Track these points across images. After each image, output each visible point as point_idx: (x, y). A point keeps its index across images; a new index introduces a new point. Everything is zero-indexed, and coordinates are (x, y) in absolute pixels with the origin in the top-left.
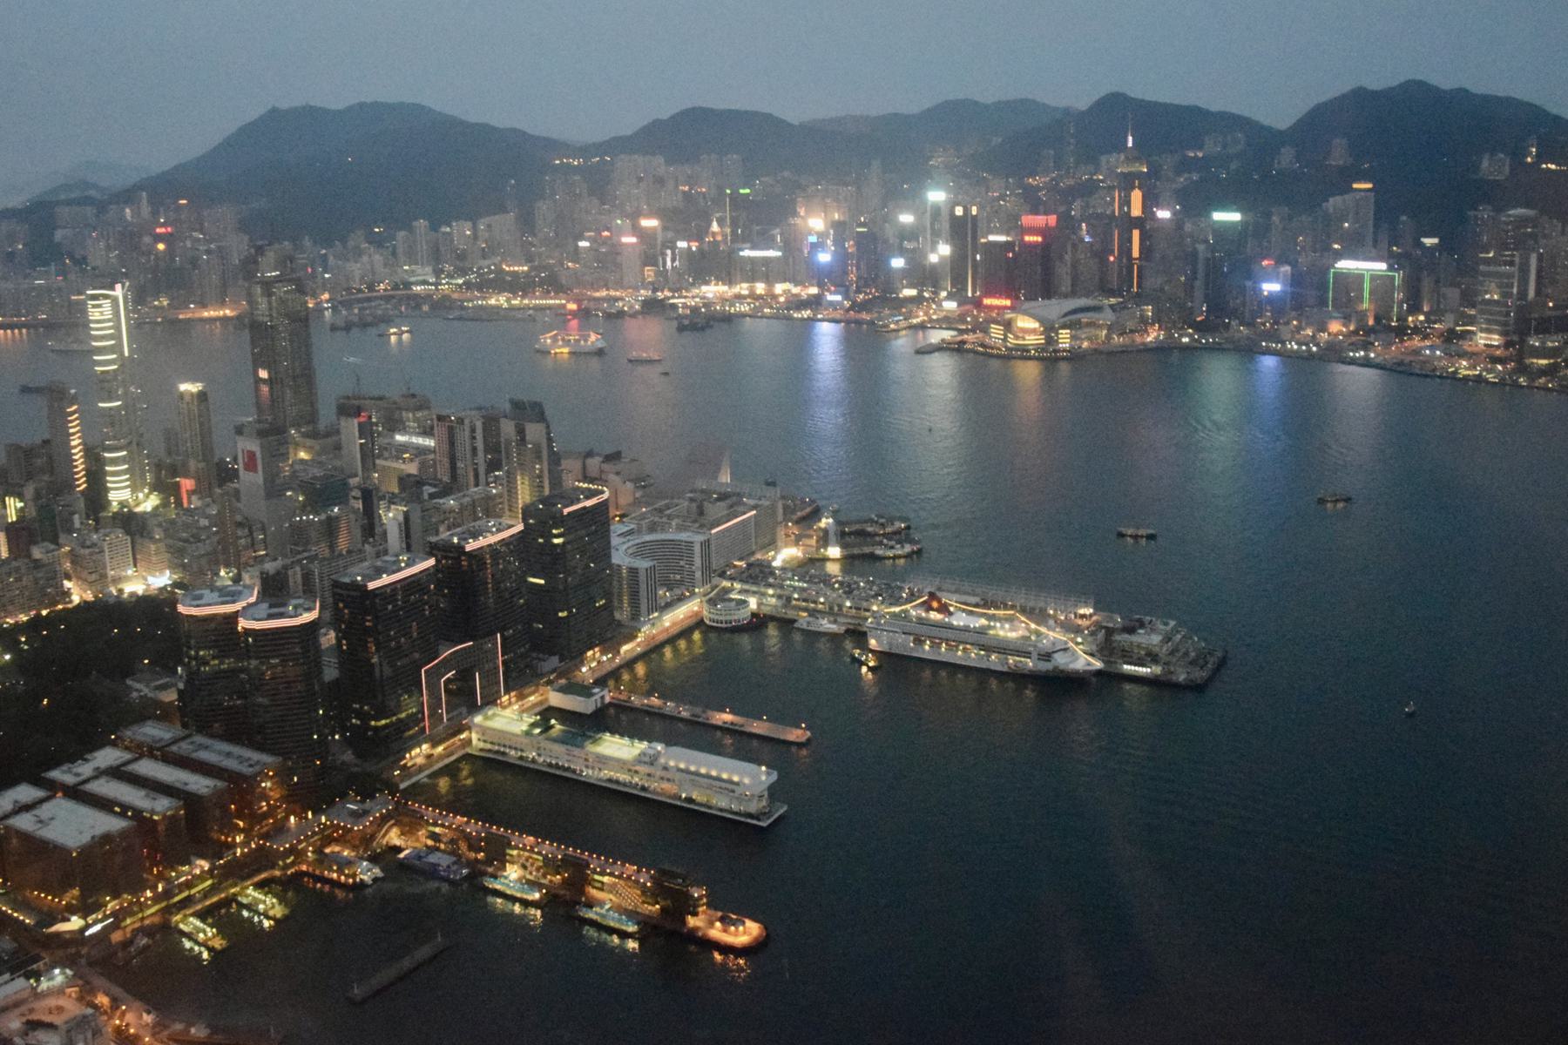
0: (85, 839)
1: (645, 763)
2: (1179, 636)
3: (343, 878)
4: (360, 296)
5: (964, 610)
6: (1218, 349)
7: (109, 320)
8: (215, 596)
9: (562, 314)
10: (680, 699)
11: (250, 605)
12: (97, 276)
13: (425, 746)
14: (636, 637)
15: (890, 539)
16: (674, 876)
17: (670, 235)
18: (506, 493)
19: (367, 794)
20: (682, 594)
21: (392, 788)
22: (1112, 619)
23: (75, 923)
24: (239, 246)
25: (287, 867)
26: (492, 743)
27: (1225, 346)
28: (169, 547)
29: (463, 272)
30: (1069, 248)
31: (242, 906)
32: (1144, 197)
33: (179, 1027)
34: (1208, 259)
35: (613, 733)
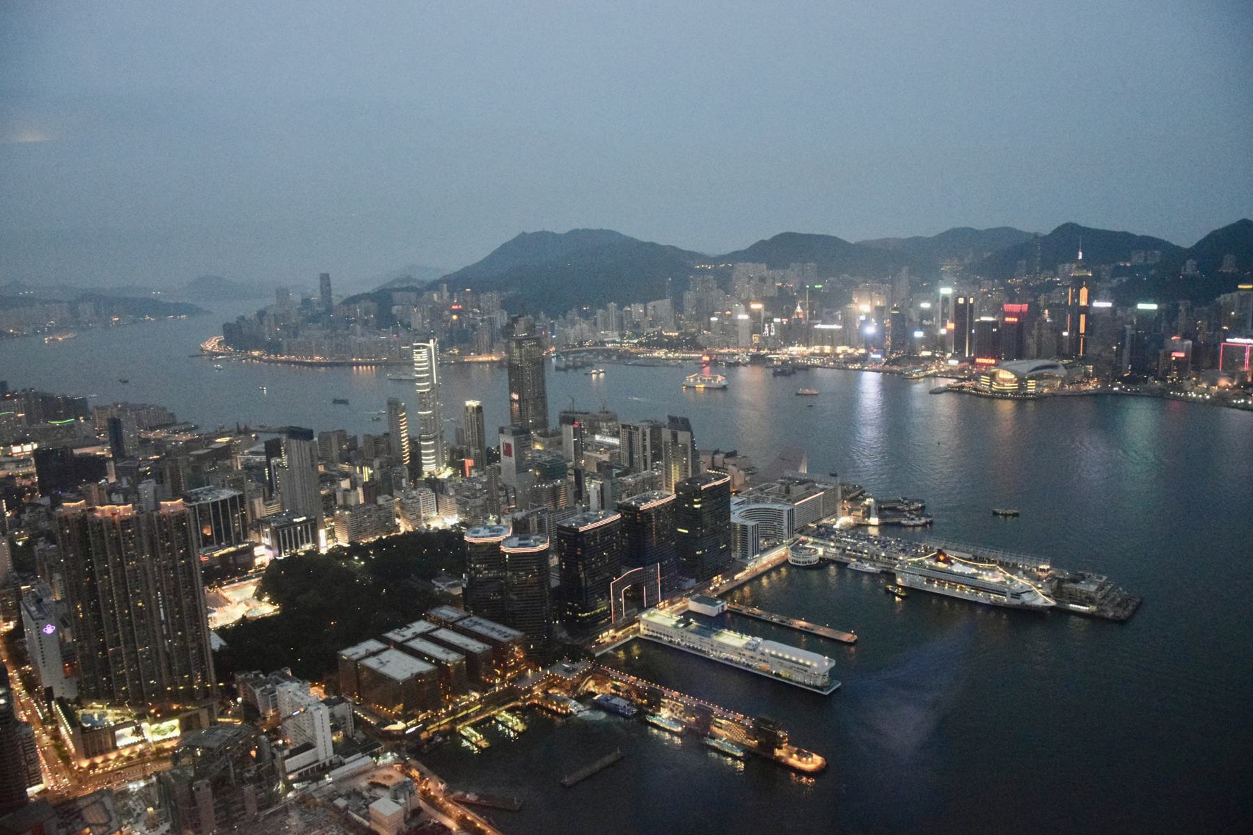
0: (407, 675)
1: (750, 650)
2: (1109, 587)
3: (559, 710)
4: (574, 349)
5: (961, 562)
6: (1137, 396)
7: (426, 361)
8: (487, 532)
9: (699, 363)
10: (772, 611)
11: (507, 538)
12: (416, 335)
13: (611, 631)
14: (745, 569)
15: (911, 514)
16: (767, 723)
17: (769, 314)
18: (664, 475)
19: (575, 659)
20: (775, 543)
21: (592, 657)
22: (1062, 574)
23: (400, 725)
24: (502, 319)
25: (525, 701)
26: (653, 631)
27: (1146, 394)
28: (458, 500)
29: (637, 337)
30: (1036, 326)
31: (498, 722)
32: (1089, 295)
33: (460, 793)
34: (1133, 335)
35: (729, 629)
